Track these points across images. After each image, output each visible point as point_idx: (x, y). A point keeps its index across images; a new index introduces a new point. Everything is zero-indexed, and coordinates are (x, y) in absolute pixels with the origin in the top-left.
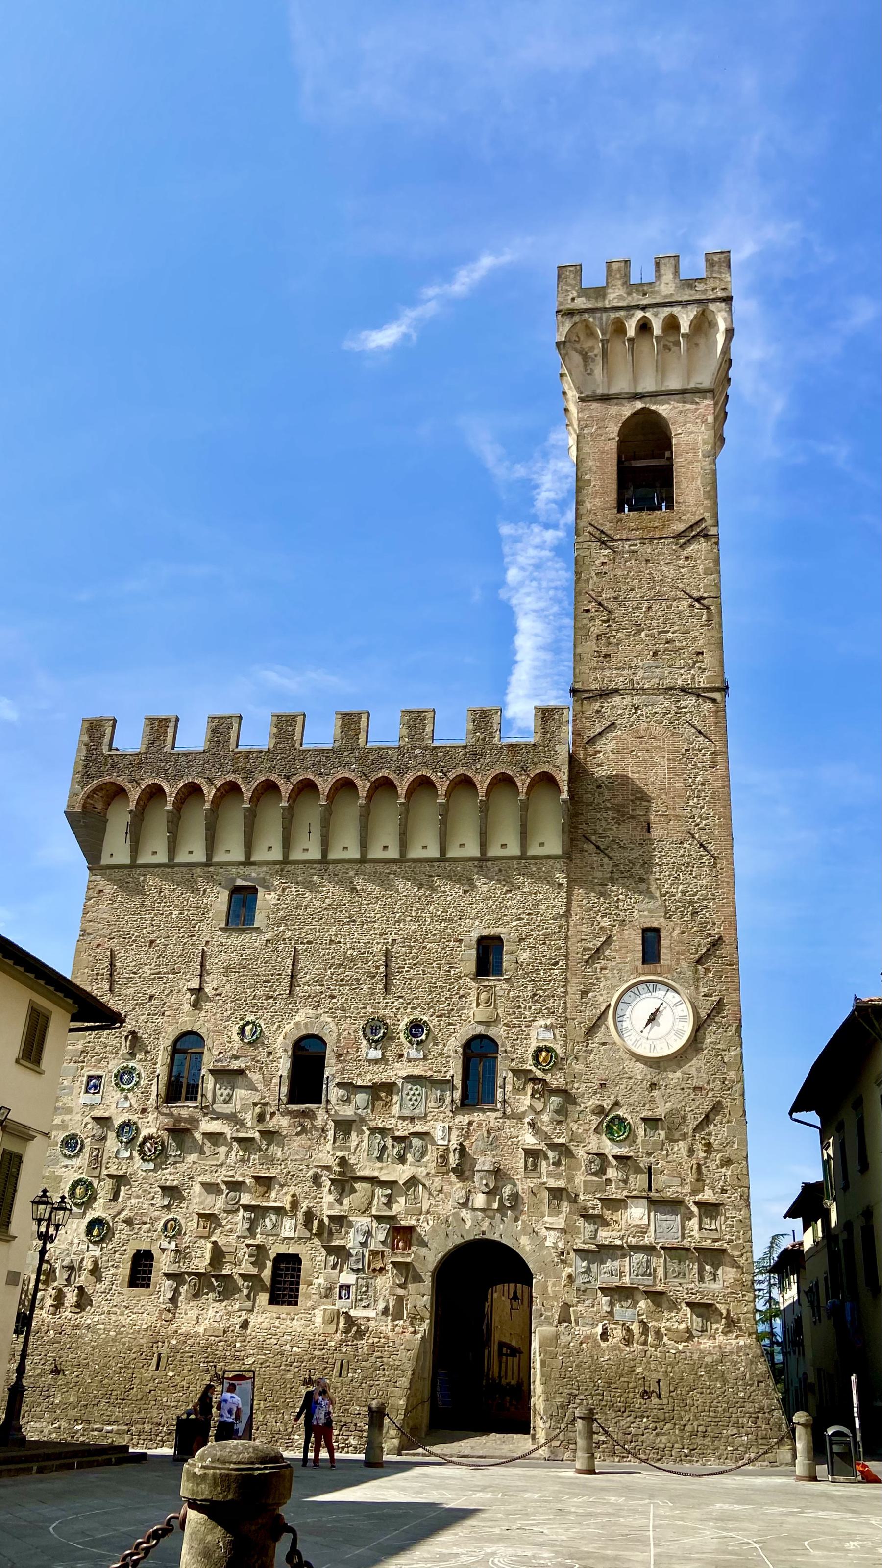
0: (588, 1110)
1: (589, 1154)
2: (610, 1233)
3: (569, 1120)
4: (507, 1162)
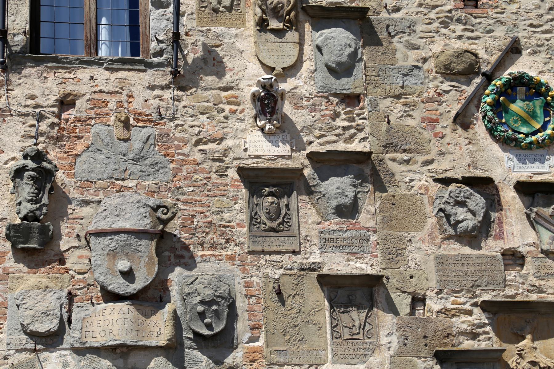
0: (431, 64)
1: (446, 182)
3: (375, 92)
4: (191, 210)
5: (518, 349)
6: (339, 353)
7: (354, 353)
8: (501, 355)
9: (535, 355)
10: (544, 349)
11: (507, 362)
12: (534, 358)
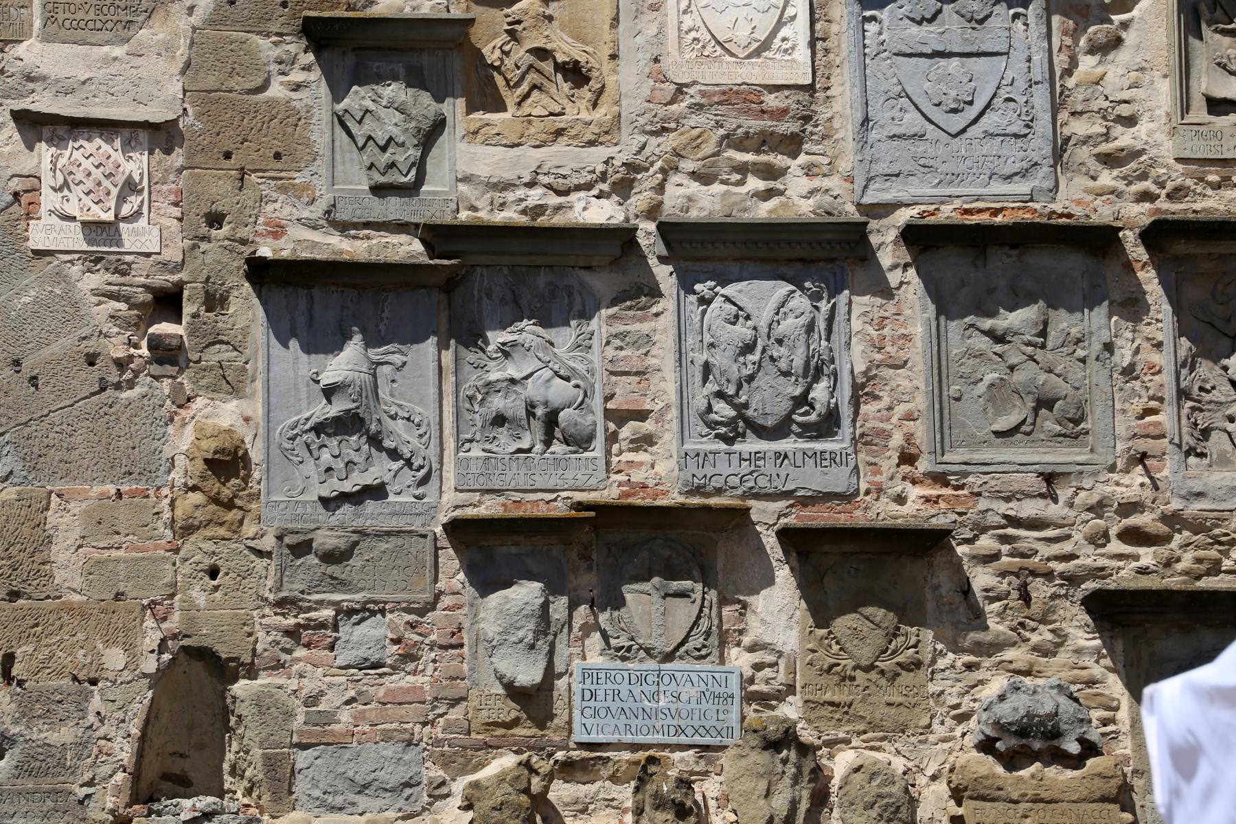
2: (530, 157)
5: (510, 19)
6: (61, 16)
7: (101, 17)
8: (467, 34)
9: (546, 33)
10: (571, 21)
11: (479, 50)
12: (544, 40)
